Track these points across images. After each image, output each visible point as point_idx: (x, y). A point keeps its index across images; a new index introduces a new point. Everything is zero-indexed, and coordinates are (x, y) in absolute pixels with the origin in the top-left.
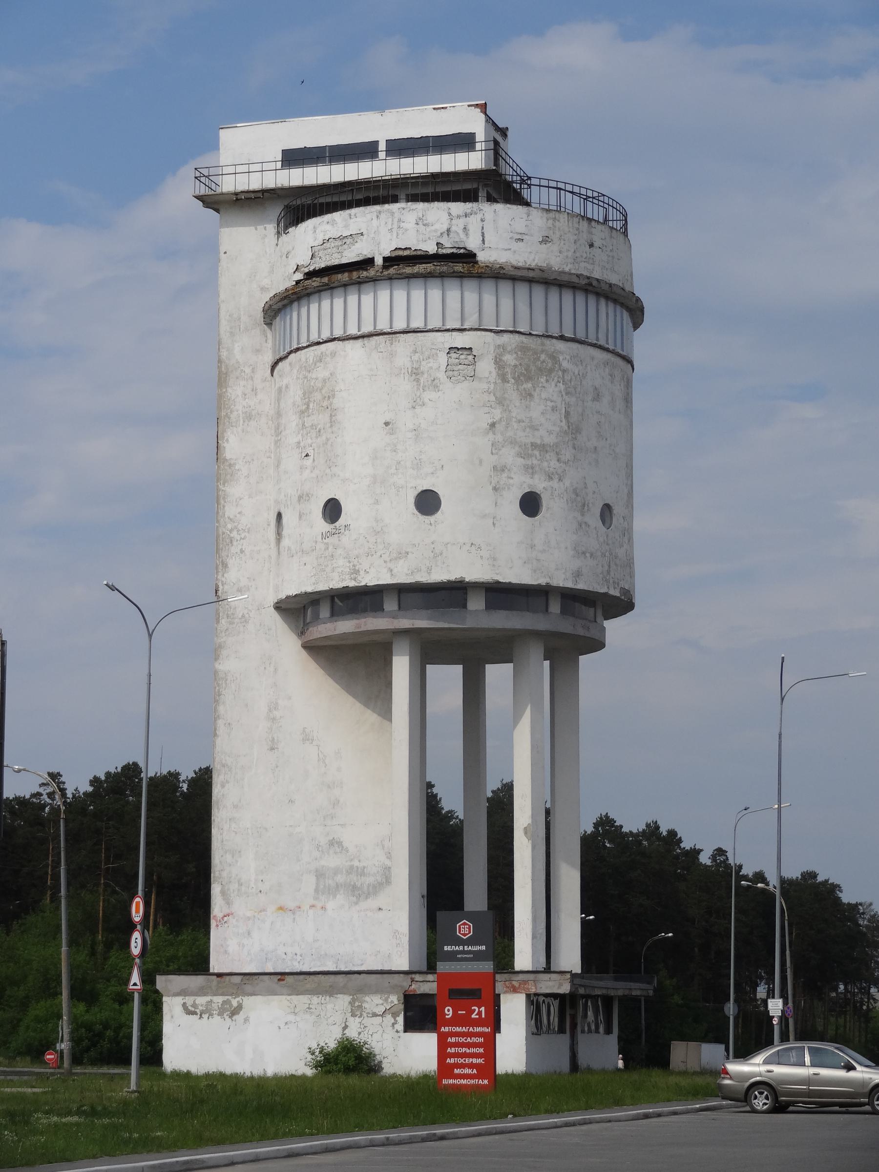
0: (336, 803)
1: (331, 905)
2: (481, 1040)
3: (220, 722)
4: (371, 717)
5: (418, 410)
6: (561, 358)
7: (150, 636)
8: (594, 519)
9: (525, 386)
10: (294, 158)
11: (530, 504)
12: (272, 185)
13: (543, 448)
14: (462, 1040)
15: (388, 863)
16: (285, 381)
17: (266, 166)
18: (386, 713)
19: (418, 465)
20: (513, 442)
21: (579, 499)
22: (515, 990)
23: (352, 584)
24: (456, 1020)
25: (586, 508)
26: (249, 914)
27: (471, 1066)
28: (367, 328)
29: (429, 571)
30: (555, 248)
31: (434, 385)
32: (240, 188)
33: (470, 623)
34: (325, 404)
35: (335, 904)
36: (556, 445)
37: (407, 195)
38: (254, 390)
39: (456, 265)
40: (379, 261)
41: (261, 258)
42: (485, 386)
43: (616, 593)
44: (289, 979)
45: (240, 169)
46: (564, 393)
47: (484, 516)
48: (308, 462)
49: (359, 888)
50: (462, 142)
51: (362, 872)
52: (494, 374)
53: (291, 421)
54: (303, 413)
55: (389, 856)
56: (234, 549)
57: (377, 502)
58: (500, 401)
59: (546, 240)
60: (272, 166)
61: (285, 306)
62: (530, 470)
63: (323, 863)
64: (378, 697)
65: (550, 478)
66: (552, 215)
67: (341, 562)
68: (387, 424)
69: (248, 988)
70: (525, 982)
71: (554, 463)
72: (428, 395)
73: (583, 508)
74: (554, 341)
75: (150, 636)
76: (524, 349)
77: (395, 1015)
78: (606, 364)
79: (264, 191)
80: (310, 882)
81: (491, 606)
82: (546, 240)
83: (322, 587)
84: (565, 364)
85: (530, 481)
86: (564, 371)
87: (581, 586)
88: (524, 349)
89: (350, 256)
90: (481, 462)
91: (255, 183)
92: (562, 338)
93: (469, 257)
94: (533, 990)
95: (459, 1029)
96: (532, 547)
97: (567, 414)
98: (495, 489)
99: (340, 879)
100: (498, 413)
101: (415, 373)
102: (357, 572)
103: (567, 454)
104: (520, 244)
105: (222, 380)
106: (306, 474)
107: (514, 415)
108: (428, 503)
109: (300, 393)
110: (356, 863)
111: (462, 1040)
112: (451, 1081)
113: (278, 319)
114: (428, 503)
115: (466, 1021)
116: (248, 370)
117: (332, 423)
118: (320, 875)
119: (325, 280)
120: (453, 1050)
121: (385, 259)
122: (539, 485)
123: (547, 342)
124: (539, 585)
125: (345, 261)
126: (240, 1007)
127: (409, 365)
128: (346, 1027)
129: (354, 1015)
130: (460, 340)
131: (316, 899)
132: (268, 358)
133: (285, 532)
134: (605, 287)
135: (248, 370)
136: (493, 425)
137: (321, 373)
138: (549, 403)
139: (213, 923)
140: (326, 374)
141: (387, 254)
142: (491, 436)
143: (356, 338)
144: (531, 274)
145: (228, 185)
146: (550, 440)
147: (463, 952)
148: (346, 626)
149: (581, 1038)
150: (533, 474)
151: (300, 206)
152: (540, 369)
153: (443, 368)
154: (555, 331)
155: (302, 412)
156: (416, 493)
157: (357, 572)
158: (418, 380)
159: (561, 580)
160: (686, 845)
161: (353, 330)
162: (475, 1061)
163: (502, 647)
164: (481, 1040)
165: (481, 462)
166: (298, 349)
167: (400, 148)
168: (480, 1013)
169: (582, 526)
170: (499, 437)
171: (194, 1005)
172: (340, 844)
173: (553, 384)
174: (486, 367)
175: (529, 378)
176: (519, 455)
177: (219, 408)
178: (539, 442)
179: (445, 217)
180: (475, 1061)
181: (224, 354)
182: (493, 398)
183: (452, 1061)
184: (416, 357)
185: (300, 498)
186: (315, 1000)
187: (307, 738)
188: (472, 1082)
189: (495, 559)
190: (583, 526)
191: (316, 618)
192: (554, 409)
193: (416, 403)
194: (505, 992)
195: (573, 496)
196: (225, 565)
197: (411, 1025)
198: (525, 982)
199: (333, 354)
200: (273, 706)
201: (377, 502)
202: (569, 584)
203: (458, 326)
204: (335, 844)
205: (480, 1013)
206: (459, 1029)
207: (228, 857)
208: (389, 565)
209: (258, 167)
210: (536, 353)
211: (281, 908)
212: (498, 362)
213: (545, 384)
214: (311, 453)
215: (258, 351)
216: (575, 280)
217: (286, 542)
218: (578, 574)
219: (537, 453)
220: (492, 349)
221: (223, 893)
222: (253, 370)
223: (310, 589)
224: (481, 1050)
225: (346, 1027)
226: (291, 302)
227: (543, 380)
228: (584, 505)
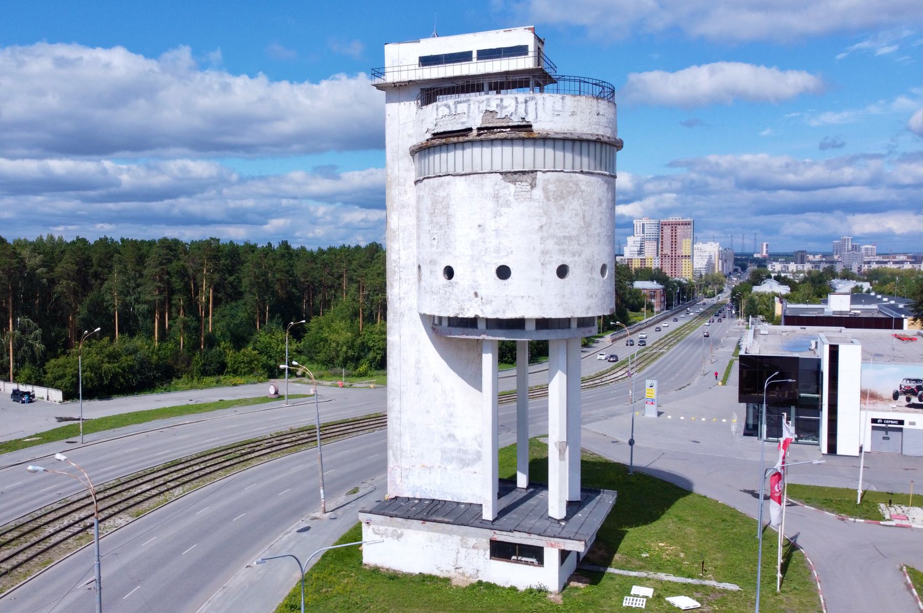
0: (451, 415)
1: (449, 467)
5: (498, 219)
12: (413, 79)
13: (570, 238)
15: (479, 449)
18: (480, 389)
19: (497, 250)
20: (554, 236)
22: (552, 546)
26: (407, 467)
29: (504, 311)
30: (578, 118)
31: (508, 204)
34: (444, 211)
36: (577, 236)
37: (490, 84)
39: (522, 133)
41: (408, 122)
42: (537, 204)
47: (537, 280)
48: (435, 243)
49: (465, 461)
51: (465, 452)
53: (426, 218)
54: (432, 214)
55: (480, 446)
56: (396, 277)
57: (474, 271)
58: (546, 213)
59: (573, 114)
62: (563, 252)
65: (574, 255)
67: (454, 303)
68: (479, 226)
71: (576, 247)
72: (504, 210)
77: (485, 550)
82: (573, 114)
84: (583, 187)
85: (562, 258)
90: (534, 249)
92: (582, 172)
98: (542, 264)
99: (454, 454)
100: (544, 220)
101: (496, 197)
102: (463, 309)
103: (584, 239)
106: (434, 249)
108: (503, 272)
109: (430, 202)
114: (503, 272)
117: (448, 223)
118: (444, 452)
121: (479, 129)
122: (566, 260)
127: (492, 192)
129: (462, 546)
133: (423, 277)
136: (541, 227)
137: (442, 193)
140: (445, 194)
142: (540, 234)
143: (462, 175)
146: (574, 233)
151: (429, 92)
152: (569, 192)
153: (512, 194)
155: (431, 214)
156: (497, 267)
161: (459, 170)
165: (534, 249)
169: (591, 280)
170: (545, 234)
172: (453, 436)
175: (563, 198)
176: (557, 243)
178: (568, 235)
179: (513, 103)
182: (541, 211)
184: (496, 188)
185: (431, 262)
186: (442, 536)
187: (436, 380)
189: (542, 305)
192: (576, 215)
193: (497, 215)
199: (449, 183)
200: (418, 362)
203: (521, 170)
204: (451, 436)
207: (396, 437)
215: (407, 170)
217: (423, 283)
219: (566, 241)
221: (394, 455)
222: (405, 181)
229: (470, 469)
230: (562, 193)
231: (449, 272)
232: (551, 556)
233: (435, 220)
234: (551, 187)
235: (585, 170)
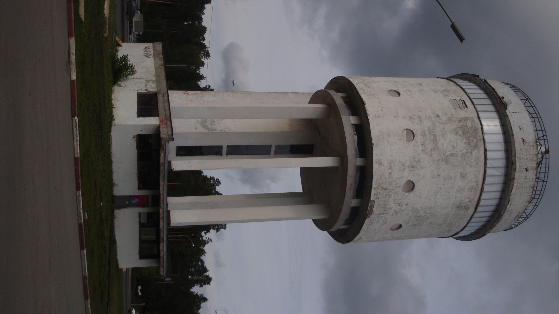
6: (476, 151)
8: (408, 176)
9: (460, 131)
13: (435, 141)
21: (416, 163)
22: (161, 121)
25: (412, 169)
46: (461, 153)
52: (460, 117)
58: (450, 120)
59: (524, 141)
65: (423, 145)
74: (483, 147)
78: (477, 182)
82: (524, 141)
84: (474, 153)
86: (471, 153)
88: (476, 130)
92: (485, 150)
93: (505, 106)
96: (389, 135)
97: (453, 155)
98: (411, 117)
100: (444, 118)
104: (518, 129)
107: (446, 126)
122: (419, 138)
124: (371, 139)
130: (468, 103)
136: (438, 116)
138: (455, 144)
150: (423, 135)
152: (469, 139)
158: (444, 91)
165: (421, 111)
173: (464, 146)
174: (462, 113)
176: (429, 128)
178: (437, 138)
182: (450, 116)
190: (403, 167)
194: (160, 119)
195: (416, 160)
198: (166, 124)
202: (375, 158)
210: (476, 136)
213: (463, 141)
220: (471, 116)
227: (465, 140)
228: (413, 167)
230: (467, 132)
234: (469, 123)
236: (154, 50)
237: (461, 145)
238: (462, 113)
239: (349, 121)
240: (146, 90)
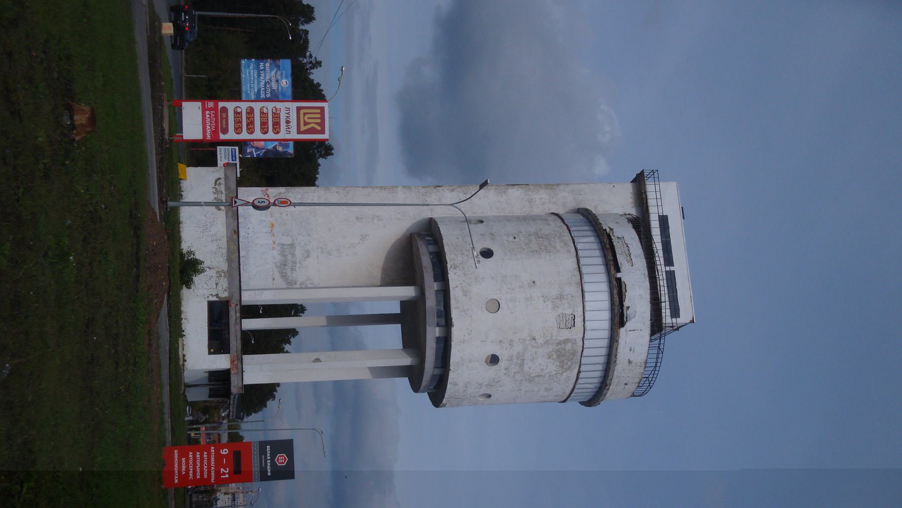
1: (275, 253)
2: (206, 477)
3: (371, 190)
4: (378, 274)
7: (451, 205)
10: (664, 221)
11: (494, 360)
13: (522, 365)
14: (205, 463)
16: (551, 223)
17: (660, 208)
22: (232, 362)
23: (449, 266)
24: (219, 457)
27: (187, 471)
28: (584, 270)
31: (555, 307)
32: (648, 194)
33: (428, 329)
35: (275, 255)
38: (544, 204)
39: (619, 318)
40: (619, 275)
43: (444, 401)
44: (235, 237)
45: (658, 194)
48: (511, 238)
49: (285, 267)
50: (675, 312)
58: (547, 343)
59: (630, 362)
60: (660, 211)
61: (590, 222)
62: (510, 359)
63: (297, 247)
64: (389, 280)
66: (643, 365)
68: (534, 282)
69: (230, 214)
70: (237, 368)
71: (514, 371)
73: (490, 385)
75: (451, 205)
76: (574, 353)
79: (647, 207)
80: (287, 241)
81: (438, 339)
82: (630, 362)
83: (446, 249)
84: (565, 374)
87: (449, 386)
88: (574, 353)
89: (621, 259)
91: (652, 202)
92: (579, 372)
93: (622, 324)
94: (232, 372)
95: (213, 459)
96: (470, 361)
98: (501, 341)
99: (289, 257)
100: (540, 341)
101: (561, 297)
105: (549, 186)
110: (298, 265)
111: (205, 463)
112: (176, 456)
113: (582, 217)
115: (219, 464)
116: (554, 200)
118: (292, 246)
119: (608, 246)
120: (198, 456)
122: (502, 364)
123: (578, 365)
125: (618, 256)
126: (220, 209)
127: (565, 293)
128: (210, 268)
129: (217, 272)
130: (579, 320)
131: (278, 244)
132: (561, 212)
134: (605, 392)
135: (554, 200)
136: (534, 339)
137: (558, 245)
139: (264, 189)
140: (558, 247)
141: (623, 279)
144: (613, 357)
145: (650, 187)
146: (526, 368)
147: (266, 460)
148: (426, 261)
149: (208, 388)
154: (583, 368)
157: (455, 268)
159: (452, 377)
160: (292, 340)
161: (582, 261)
162: (191, 472)
163: (413, 340)
164: (206, 477)
165: (515, 333)
166: (570, 231)
167: (671, 276)
168: (224, 474)
170: (527, 342)
171: (220, 184)
172: (308, 256)
174: (565, 334)
175: (558, 357)
176: (518, 353)
177: (534, 185)
180: (191, 472)
181: (562, 187)
183: (191, 456)
185: (492, 234)
186: (224, 251)
188: (176, 472)
191: (428, 243)
192: (542, 370)
196: (453, 190)
197: (211, 304)
198: (237, 368)
199: (569, 251)
201: (493, 278)
202: (450, 380)
204: (308, 254)
205: (224, 474)
206: (213, 459)
208: (459, 287)
209: (659, 204)
211: (273, 225)
212: (566, 341)
214: (517, 240)
216: (610, 378)
218: (455, 384)
223: (444, 242)
224: (198, 477)
225: (210, 268)
226: (593, 226)
227: (558, 363)
229: (277, 276)
231: (487, 254)
232: (222, 362)
233: (533, 238)
234: (569, 346)
235: (581, 375)
236: (226, 185)
237: (552, 367)
238: (565, 334)
239: (433, 332)
240: (217, 295)
